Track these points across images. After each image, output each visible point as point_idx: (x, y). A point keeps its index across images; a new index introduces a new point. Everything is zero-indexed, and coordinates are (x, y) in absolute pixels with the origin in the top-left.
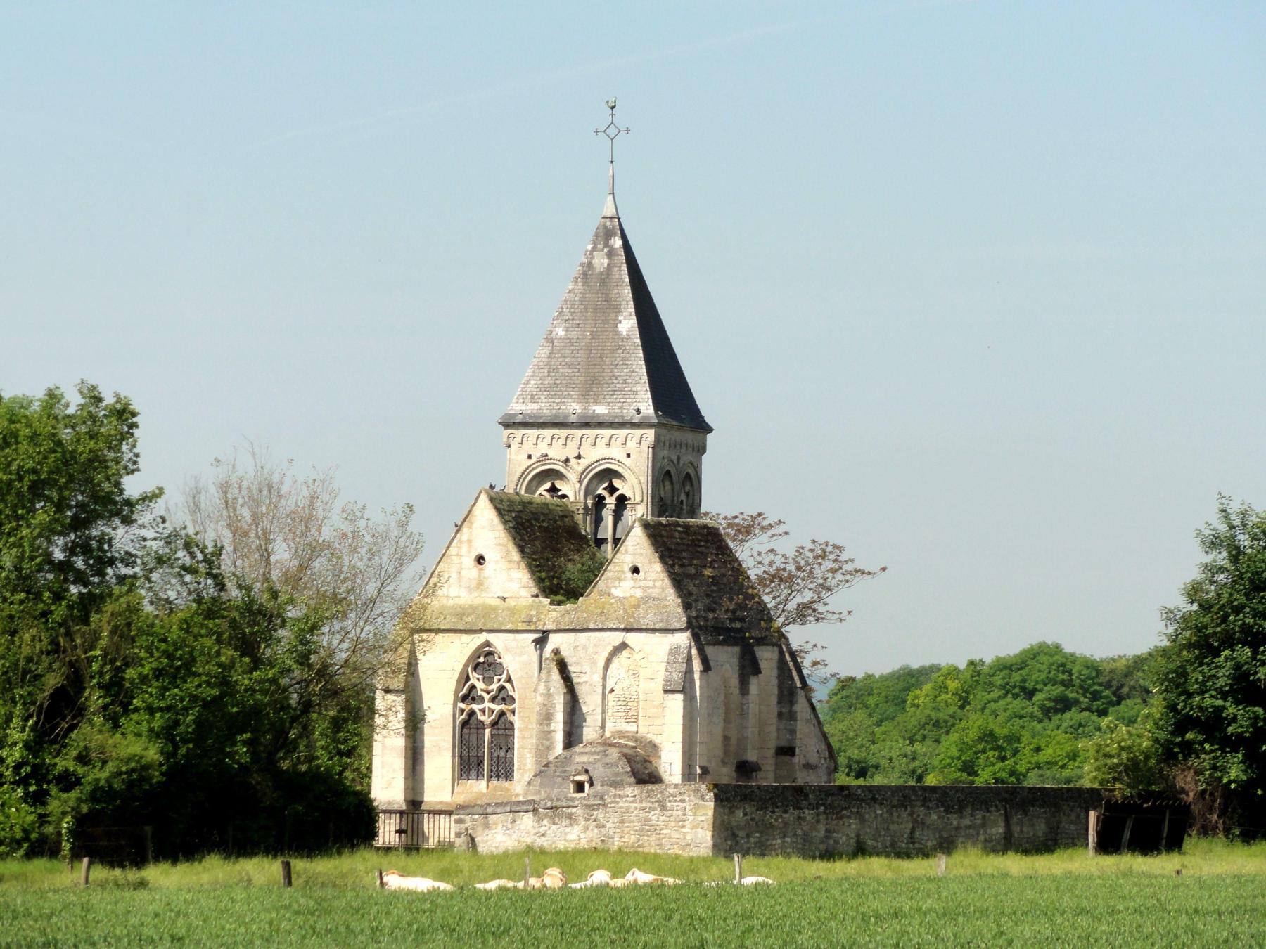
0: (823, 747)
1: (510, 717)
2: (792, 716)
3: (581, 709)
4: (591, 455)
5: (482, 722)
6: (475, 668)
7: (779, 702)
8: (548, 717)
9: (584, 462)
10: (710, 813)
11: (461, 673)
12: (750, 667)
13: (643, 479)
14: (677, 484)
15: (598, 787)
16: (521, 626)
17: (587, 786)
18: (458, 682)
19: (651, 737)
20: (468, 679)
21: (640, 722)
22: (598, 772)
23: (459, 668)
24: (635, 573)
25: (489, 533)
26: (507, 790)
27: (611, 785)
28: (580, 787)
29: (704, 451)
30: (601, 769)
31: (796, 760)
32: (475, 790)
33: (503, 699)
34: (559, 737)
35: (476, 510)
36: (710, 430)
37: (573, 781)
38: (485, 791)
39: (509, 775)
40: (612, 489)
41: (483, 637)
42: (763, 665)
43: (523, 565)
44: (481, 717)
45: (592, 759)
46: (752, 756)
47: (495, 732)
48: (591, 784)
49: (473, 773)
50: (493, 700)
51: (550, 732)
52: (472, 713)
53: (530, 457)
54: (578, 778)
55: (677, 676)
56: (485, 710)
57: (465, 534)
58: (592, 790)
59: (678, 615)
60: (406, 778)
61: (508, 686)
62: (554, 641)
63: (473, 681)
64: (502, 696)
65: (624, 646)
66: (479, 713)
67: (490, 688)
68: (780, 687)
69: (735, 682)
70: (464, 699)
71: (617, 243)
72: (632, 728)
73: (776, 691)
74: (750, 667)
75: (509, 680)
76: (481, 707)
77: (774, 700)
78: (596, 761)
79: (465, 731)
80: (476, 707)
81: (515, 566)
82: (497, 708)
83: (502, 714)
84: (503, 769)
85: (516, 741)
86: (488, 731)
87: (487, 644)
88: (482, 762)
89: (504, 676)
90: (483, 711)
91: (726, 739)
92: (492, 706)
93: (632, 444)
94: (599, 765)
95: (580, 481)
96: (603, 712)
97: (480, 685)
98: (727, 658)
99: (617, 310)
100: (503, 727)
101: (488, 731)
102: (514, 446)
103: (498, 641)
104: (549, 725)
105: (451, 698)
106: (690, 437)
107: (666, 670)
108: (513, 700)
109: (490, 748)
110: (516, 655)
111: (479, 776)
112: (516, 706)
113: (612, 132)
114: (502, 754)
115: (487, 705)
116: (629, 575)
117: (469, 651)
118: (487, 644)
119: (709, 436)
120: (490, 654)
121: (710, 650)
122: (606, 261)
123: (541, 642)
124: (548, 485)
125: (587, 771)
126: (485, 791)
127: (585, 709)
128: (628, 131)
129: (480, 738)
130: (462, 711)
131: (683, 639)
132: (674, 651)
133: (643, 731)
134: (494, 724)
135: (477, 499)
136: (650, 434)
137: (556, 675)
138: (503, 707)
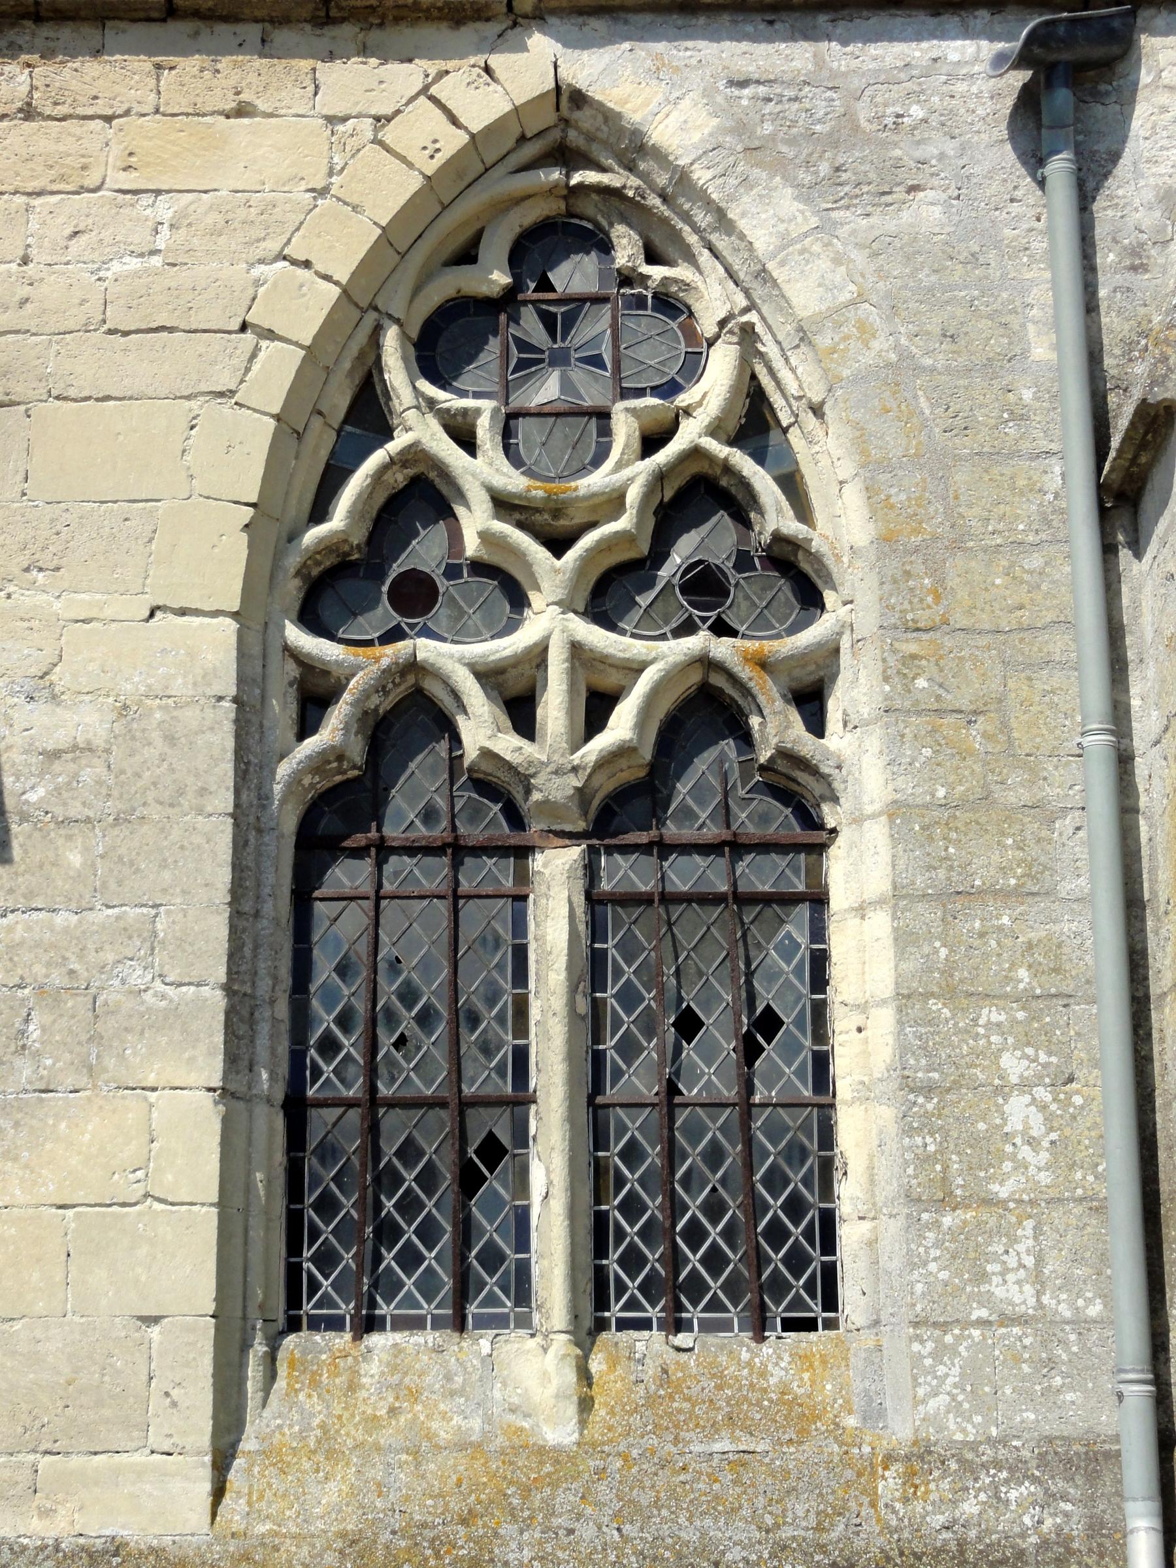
5: (496, 787)
6: (442, 347)
18: (289, 429)
20: (369, 415)
23: (306, 309)
26: (799, 1417)
32: (456, 1421)
33: (704, 585)
38: (560, 1432)
47: (623, 873)
50: (608, 594)
52: (414, 715)
63: (417, 430)
64: (713, 538)
70: (327, 592)
75: (753, 421)
79: (349, 875)
83: (706, 711)
84: (726, 1226)
86: (556, 869)
87: (565, 129)
89: (713, 387)
97: (482, 472)
100: (712, 825)
101: (556, 869)
105: (218, 563)
108: (799, 579)
109: (591, 1023)
111: (478, 1284)
114: (709, 1071)
117: (387, 190)
118: (565, 129)
126: (560, 1432)
134: (621, 812)
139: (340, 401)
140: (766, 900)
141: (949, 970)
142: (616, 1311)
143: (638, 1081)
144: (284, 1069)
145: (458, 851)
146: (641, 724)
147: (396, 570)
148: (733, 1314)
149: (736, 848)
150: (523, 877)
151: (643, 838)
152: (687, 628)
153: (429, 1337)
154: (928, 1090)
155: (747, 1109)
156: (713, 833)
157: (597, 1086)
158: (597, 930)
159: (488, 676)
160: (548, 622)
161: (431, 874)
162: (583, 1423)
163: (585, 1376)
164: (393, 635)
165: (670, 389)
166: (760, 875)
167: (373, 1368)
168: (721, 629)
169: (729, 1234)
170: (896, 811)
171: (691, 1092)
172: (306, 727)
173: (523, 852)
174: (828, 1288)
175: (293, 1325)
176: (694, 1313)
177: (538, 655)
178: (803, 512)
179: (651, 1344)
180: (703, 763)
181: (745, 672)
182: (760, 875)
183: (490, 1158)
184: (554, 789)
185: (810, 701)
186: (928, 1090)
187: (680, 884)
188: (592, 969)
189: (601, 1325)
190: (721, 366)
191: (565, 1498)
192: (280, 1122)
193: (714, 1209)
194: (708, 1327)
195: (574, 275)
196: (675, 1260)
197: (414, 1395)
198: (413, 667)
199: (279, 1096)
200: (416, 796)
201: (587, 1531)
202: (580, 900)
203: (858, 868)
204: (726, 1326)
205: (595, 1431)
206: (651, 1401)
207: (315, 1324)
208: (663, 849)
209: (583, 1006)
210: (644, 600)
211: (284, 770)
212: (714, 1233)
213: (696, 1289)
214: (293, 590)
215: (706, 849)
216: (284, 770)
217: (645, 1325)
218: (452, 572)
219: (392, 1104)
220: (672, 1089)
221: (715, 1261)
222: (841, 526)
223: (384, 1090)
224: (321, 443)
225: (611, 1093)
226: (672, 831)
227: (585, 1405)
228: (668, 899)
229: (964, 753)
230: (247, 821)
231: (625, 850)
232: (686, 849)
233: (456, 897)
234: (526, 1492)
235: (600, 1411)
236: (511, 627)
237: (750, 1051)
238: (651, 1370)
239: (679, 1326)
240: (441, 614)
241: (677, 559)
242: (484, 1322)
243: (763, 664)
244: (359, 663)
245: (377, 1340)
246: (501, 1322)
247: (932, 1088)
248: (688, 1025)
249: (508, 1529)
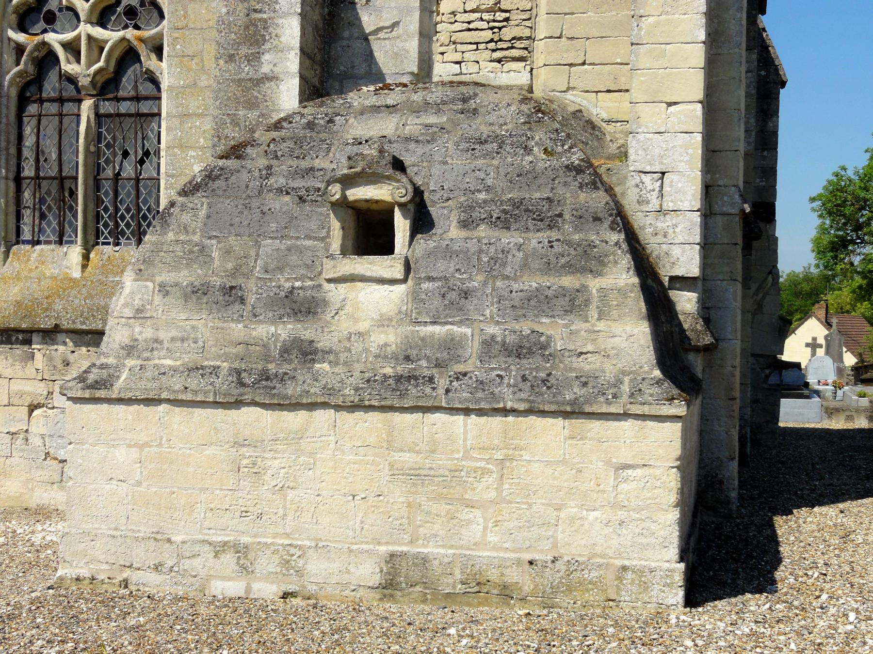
1: (149, 61)
3: (356, 22)
5: (71, 80)
8: (254, 35)
15: (449, 228)
17: (401, 225)
19: (575, 100)
21: (539, 58)
22: (444, 170)
27: (504, 222)
28: (370, 233)
30: (459, 162)
32: (51, 270)
37: (343, 206)
44: (69, 67)
45: (413, 126)
47: (107, 107)
48: (422, 222)
51: (259, 82)
52: (46, 59)
58: (423, 243)
72: (515, 75)
76: (69, 36)
78: (432, 134)
79: (33, 109)
82: (110, 36)
83: (128, 56)
86: (87, 105)
88: (73, 193)
90: (72, 48)
92: (98, 32)
94: (448, 143)
96: (427, 34)
101: (87, 105)
104: (254, 59)
114: (129, 170)
125: (398, 165)
126: (76, 274)
127: (368, 21)
129: (65, 123)
130: (20, 49)
133: (547, 82)
134: (106, 86)
138: (130, 33)
140: (147, 115)
141: (181, 138)
142: (101, 240)
143: (109, 173)
144: (14, 169)
145: (61, 100)
146: (107, 61)
147: (45, 9)
148: (133, 241)
149: (137, 99)
150: (79, 109)
151: (111, 96)
152: (126, 27)
153: (52, 246)
154: (172, 176)
155: (138, 180)
156: (132, 93)
157: (98, 174)
158: (99, 125)
159: (66, 46)
161: (52, 108)
162: (83, 272)
163: (86, 257)
164: (45, 31)
167: (34, 255)
168: (137, 27)
169: (131, 218)
170: (170, 88)
171: (124, 175)
172: (18, 64)
173: (80, 101)
175: (18, 243)
176: (122, 241)
177: (78, 38)
179: (108, 249)
180: (130, 71)
181: (135, 43)
182: (145, 107)
184: (84, 82)
185: (159, 51)
186: (172, 176)
187: (123, 110)
188: (95, 137)
189: (98, 244)
191: (74, 292)
192: (12, 185)
193: (128, 210)
194: (125, 245)
196: (117, 225)
197: (43, 263)
198: (44, 43)
199: (12, 175)
200: (51, 86)
201: (77, 301)
202: (92, 117)
204: (131, 244)
205: (86, 274)
206: (103, 266)
207: (24, 242)
208: (118, 100)
209: (92, 149)
210: (113, 18)
211: (8, 77)
212: (128, 217)
213: (123, 233)
214: (13, 18)
215: (131, 99)
216: (8, 77)
217: (109, 244)
218: (60, 10)
219: (44, 178)
220: (119, 174)
221: (128, 225)
223: (42, 174)
225: (102, 176)
226: (121, 94)
227: (84, 267)
228: (119, 115)
229: (190, 70)
231: (108, 100)
232: (125, 99)
233: (61, 115)
234: (64, 290)
235: (89, 268)
236: (77, 27)
237: (142, 162)
238: (106, 256)
239: (117, 244)
240: (58, 25)
242: (67, 242)
243: (141, 40)
245: (38, 247)
246: (71, 242)
248: (126, 154)
249: (57, 300)
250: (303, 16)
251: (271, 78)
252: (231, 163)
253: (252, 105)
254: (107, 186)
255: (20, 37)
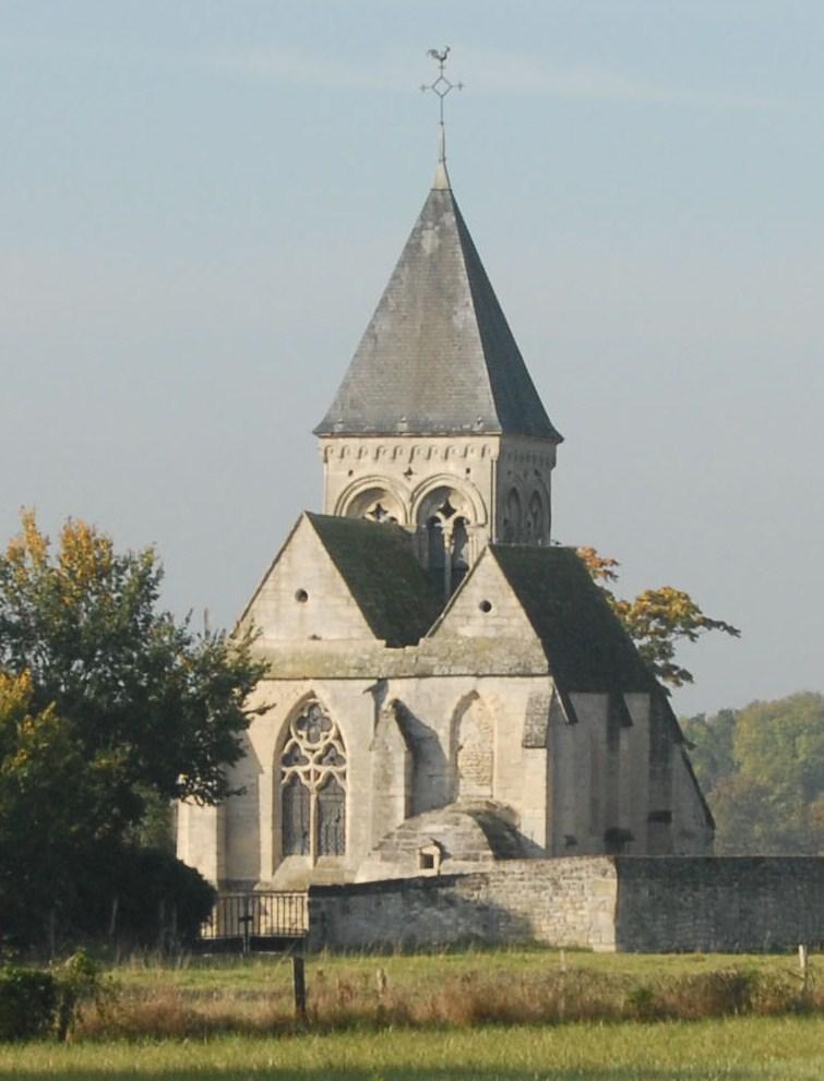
0: (700, 809)
2: (667, 773)
4: (424, 470)
7: (651, 759)
9: (416, 479)
10: (613, 891)
11: (282, 730)
12: (619, 718)
13: (487, 498)
14: (523, 500)
16: (353, 673)
18: (279, 739)
24: (488, 610)
25: (311, 560)
26: (337, 866)
29: (554, 464)
31: (673, 825)
33: (332, 759)
34: (400, 804)
35: (296, 539)
36: (560, 439)
39: (339, 849)
40: (448, 511)
41: (309, 685)
42: (634, 716)
43: (353, 600)
46: (623, 823)
49: (297, 848)
50: (319, 761)
52: (295, 776)
53: (351, 473)
54: (425, 851)
55: (539, 730)
56: (310, 771)
57: (283, 567)
59: (539, 658)
60: (218, 854)
61: (336, 743)
62: (397, 689)
64: (331, 756)
65: (474, 695)
66: (337, 777)
67: (315, 746)
68: (652, 741)
69: (601, 731)
71: (450, 219)
72: (486, 791)
73: (648, 746)
74: (619, 718)
75: (339, 737)
76: (306, 768)
77: (646, 757)
80: (300, 769)
81: (345, 602)
82: (324, 770)
83: (330, 777)
85: (348, 808)
87: (312, 695)
89: (333, 732)
90: (307, 774)
91: (594, 803)
92: (319, 768)
93: (473, 457)
95: (412, 500)
97: (304, 744)
98: (592, 706)
99: (452, 298)
102: (333, 459)
103: (324, 693)
104: (388, 789)
106: (536, 448)
107: (526, 724)
108: (342, 761)
110: (347, 708)
112: (347, 767)
113: (442, 87)
115: (311, 766)
116: (479, 612)
118: (312, 695)
119: (559, 447)
120: (315, 705)
121: (575, 698)
122: (437, 241)
123: (378, 690)
124: (373, 508)
128: (460, 86)
131: (544, 686)
132: (534, 701)
135: (297, 526)
136: (493, 445)
137: (394, 728)
139: (286, 732)
160: (311, 766)
165: (328, 730)
166: (339, 798)
168: (335, 765)
174: (344, 850)
178: (344, 750)
182: (339, 798)
183: (306, 834)
185: (343, 775)
190: (334, 729)
195: (315, 712)
203: (348, 799)
222: (348, 756)
224: (284, 739)
230: (275, 793)
241: (330, 754)
244: (288, 770)
247: (354, 824)
250: (406, 774)
251: (392, 796)
252: (387, 840)
253: (386, 806)
254: (323, 830)
255: (284, 769)
